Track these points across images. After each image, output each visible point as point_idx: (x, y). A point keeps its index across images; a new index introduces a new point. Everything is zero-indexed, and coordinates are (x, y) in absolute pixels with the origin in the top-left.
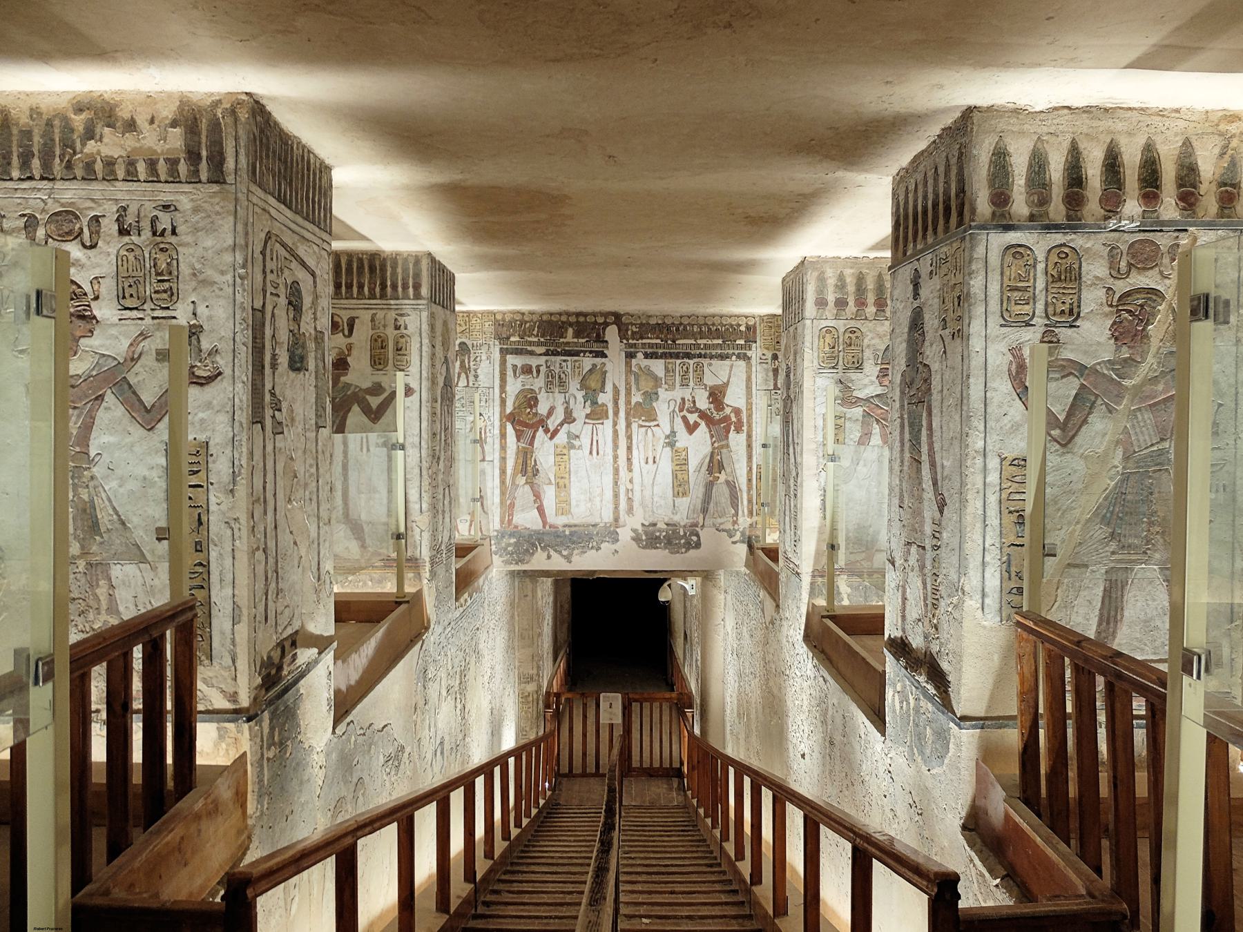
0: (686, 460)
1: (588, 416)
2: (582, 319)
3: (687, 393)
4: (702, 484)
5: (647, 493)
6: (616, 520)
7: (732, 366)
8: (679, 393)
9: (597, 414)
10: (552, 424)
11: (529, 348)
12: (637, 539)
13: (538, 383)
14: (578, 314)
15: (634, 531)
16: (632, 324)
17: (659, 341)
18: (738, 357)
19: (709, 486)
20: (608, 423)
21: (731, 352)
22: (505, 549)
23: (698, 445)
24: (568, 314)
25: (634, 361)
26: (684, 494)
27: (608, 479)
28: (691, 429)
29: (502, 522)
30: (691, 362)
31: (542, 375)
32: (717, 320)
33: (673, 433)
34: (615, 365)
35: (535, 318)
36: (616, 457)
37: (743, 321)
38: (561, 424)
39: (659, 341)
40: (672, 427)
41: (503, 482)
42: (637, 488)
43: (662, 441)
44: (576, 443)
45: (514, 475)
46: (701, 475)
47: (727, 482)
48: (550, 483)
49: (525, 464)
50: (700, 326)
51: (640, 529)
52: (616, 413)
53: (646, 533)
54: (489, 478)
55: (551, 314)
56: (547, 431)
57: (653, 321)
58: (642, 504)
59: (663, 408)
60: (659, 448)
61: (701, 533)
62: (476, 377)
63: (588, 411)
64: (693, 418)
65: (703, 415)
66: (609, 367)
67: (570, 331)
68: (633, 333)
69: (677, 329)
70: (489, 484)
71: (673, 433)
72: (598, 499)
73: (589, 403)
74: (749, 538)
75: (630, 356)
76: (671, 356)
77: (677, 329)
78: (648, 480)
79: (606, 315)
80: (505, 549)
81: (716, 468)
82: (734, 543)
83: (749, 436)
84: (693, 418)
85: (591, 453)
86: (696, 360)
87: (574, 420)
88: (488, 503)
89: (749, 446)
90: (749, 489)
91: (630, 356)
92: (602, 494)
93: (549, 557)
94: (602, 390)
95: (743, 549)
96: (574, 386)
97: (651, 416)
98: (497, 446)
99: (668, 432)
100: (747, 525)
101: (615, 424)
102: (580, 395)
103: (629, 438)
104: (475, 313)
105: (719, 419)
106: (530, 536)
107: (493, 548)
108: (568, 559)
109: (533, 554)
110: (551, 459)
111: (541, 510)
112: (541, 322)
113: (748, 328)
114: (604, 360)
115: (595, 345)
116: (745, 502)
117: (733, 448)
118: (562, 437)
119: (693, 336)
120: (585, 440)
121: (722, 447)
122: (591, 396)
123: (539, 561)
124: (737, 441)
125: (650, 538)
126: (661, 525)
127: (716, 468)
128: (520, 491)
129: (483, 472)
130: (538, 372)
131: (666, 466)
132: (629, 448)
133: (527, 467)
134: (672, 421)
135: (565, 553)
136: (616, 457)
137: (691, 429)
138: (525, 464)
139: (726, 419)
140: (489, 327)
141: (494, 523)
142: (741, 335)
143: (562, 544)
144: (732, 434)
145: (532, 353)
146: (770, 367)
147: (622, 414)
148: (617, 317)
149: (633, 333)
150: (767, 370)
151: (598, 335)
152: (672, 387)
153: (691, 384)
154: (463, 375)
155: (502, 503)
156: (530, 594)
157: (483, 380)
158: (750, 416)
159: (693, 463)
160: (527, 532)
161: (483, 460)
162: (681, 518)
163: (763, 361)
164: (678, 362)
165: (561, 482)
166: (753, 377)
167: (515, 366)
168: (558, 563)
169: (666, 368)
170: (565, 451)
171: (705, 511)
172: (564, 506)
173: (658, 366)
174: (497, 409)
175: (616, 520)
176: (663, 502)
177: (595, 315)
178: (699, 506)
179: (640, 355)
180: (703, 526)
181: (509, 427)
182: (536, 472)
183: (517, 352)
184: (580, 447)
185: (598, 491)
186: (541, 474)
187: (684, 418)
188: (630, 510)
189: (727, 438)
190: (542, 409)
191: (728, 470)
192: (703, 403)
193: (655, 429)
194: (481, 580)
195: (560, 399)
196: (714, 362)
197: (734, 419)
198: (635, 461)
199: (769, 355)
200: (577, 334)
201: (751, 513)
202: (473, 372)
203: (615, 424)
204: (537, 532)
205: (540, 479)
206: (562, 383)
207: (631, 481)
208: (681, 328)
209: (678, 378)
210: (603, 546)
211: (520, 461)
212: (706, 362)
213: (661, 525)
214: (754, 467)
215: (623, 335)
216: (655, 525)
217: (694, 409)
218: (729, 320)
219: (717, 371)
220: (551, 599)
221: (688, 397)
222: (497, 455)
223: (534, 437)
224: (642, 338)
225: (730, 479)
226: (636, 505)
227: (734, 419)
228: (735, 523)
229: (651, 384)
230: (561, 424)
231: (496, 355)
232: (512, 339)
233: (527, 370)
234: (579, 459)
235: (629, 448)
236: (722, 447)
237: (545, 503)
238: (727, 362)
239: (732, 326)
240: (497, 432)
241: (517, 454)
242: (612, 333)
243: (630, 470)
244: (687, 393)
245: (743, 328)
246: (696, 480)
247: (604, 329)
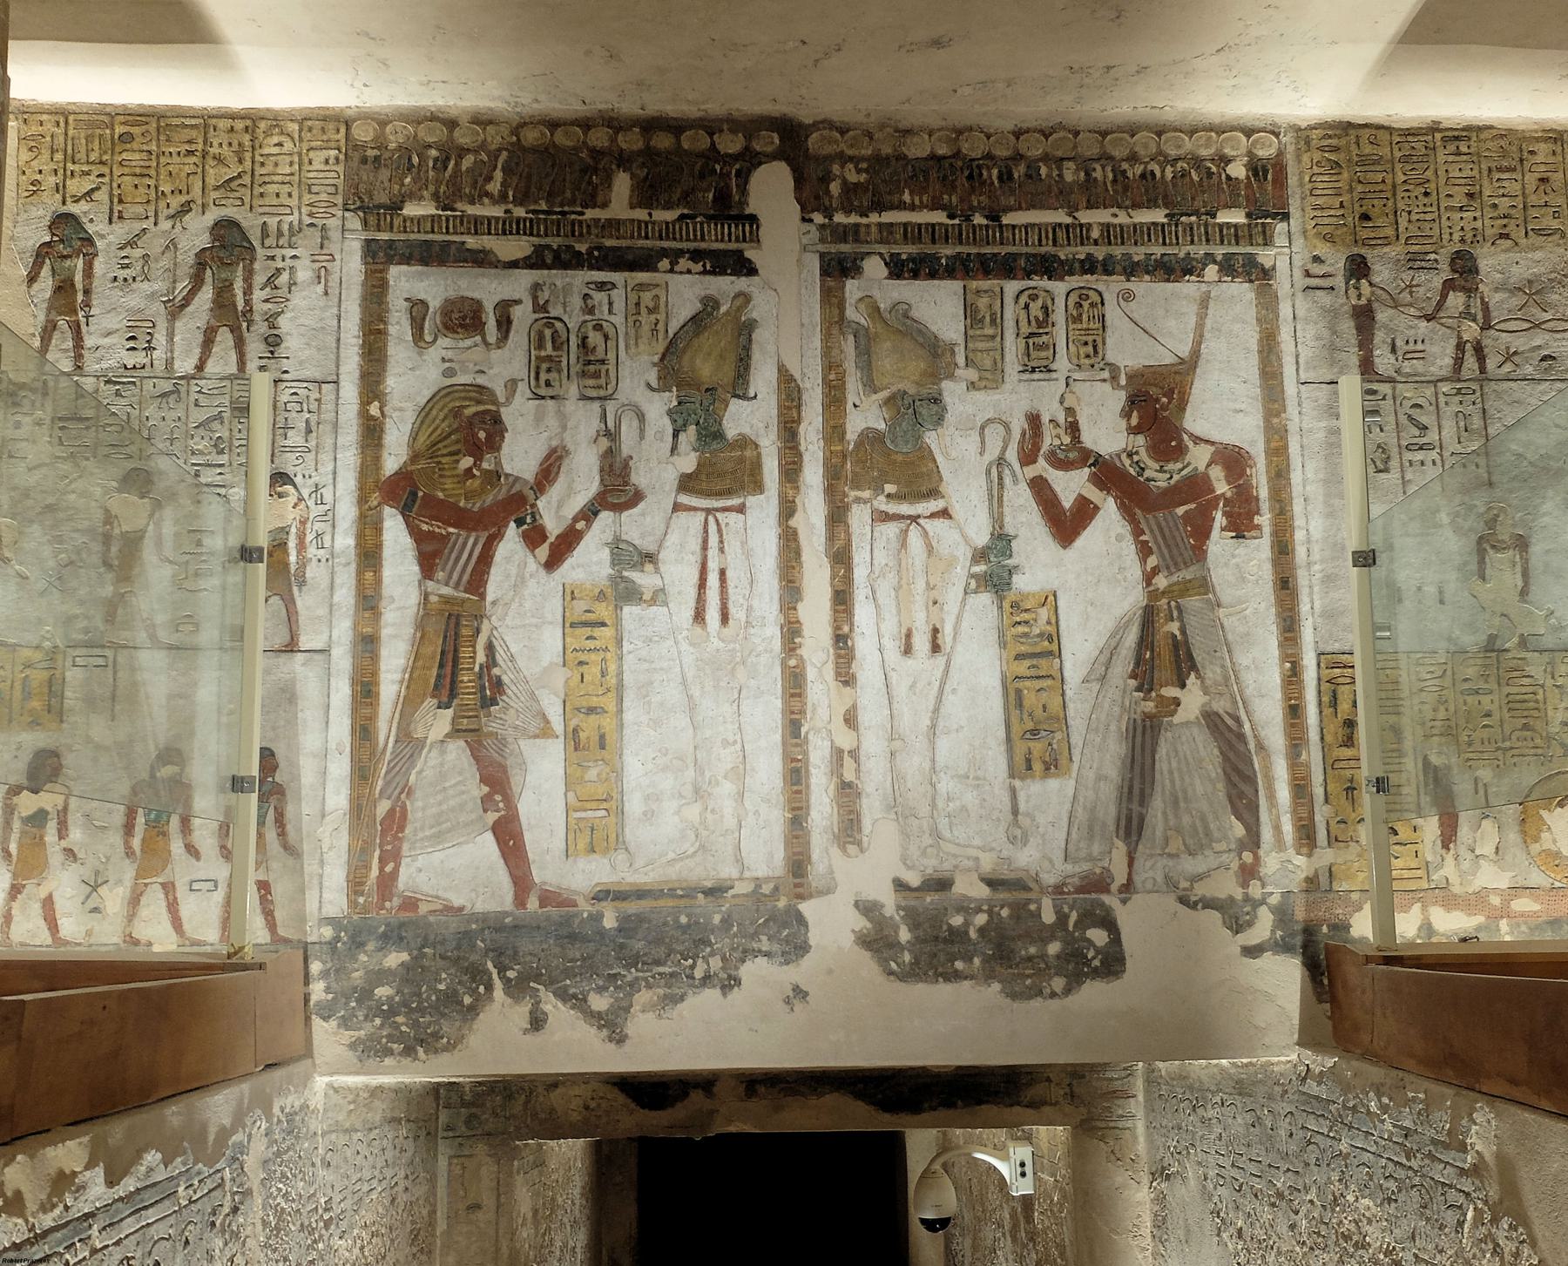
0: (1054, 637)
1: (687, 483)
2: (663, 141)
3: (1047, 399)
4: (1118, 727)
5: (914, 764)
6: (798, 865)
7: (1204, 302)
8: (1016, 397)
9: (721, 475)
10: (554, 511)
11: (471, 242)
12: (877, 942)
13: (505, 365)
14: (650, 125)
15: (867, 908)
16: (843, 159)
17: (939, 217)
18: (1228, 268)
19: (1144, 735)
20: (763, 508)
21: (1200, 250)
22: (365, 994)
23: (1094, 584)
24: (615, 124)
25: (853, 289)
26: (1052, 766)
27: (766, 712)
28: (1067, 524)
29: (355, 884)
30: (1059, 288)
31: (518, 336)
32: (1144, 144)
33: (1001, 541)
34: (783, 304)
35: (495, 137)
36: (792, 632)
37: (1237, 147)
38: (589, 514)
39: (939, 217)
40: (998, 519)
41: (363, 731)
42: (873, 745)
43: (960, 572)
44: (644, 579)
45: (409, 704)
46: (1112, 693)
47: (1212, 720)
48: (546, 732)
49: (450, 660)
50: (1085, 165)
51: (889, 901)
52: (791, 471)
53: (913, 918)
54: (308, 713)
55: (553, 124)
56: (534, 536)
57: (918, 149)
58: (897, 807)
59: (961, 450)
60: (953, 595)
61: (1125, 917)
62: (273, 342)
63: (688, 462)
64: (1071, 485)
65: (1107, 474)
66: (762, 307)
67: (622, 184)
68: (849, 189)
69: (1006, 177)
70: (310, 740)
71: (1001, 541)
72: (728, 787)
73: (689, 436)
74: (1309, 931)
75: (838, 269)
76: (989, 267)
77: (1006, 177)
78: (913, 718)
79: (750, 126)
80: (365, 994)
81: (1165, 671)
82: (1252, 952)
83: (1283, 549)
84: (1071, 485)
85: (699, 616)
86: (1075, 281)
87: (637, 497)
88: (302, 810)
89: (1285, 584)
90: (1296, 742)
91: (838, 269)
92: (740, 772)
93: (537, 1022)
94: (739, 386)
95: (1282, 982)
96: (635, 375)
97: (919, 480)
98: (345, 595)
99: (982, 539)
100: (1295, 882)
101: (788, 509)
102: (658, 408)
103: (841, 558)
104: (275, 120)
105: (1169, 494)
106: (466, 937)
107: (318, 990)
108: (612, 1026)
109: (473, 1011)
110: (551, 641)
111: (509, 836)
112: (517, 150)
113: (1257, 169)
114: (742, 283)
115: (712, 230)
116: (1284, 794)
117: (1225, 593)
118: (590, 561)
119: (1062, 196)
120: (678, 571)
121: (1185, 589)
122: (699, 409)
123: (505, 1040)
124: (1237, 565)
125: (929, 937)
126: (970, 888)
127: (1165, 671)
128: (427, 766)
129: (286, 696)
130: (505, 323)
131: (979, 662)
132: (842, 599)
133: (457, 668)
134: (996, 498)
135: (599, 1003)
136: (792, 632)
137: (1067, 524)
138: (450, 660)
139: (1195, 487)
140: (325, 167)
141: (326, 891)
142: (1232, 193)
143: (589, 967)
144: (1219, 544)
145: (481, 260)
146: (1344, 301)
147: (813, 475)
148: (791, 139)
149: (849, 189)
150: (1332, 314)
151: (723, 198)
152: (991, 378)
153: (1062, 364)
154: (224, 338)
155: (359, 809)
156: (488, 1200)
157: (300, 352)
158: (1280, 475)
159: (1080, 649)
160: (454, 924)
161: (291, 648)
162: (1045, 856)
163: (1314, 283)
164: (1011, 287)
165: (589, 727)
166: (1285, 335)
167: (417, 309)
168: (570, 1045)
169: (970, 311)
170: (603, 611)
171: (1131, 828)
172: (598, 820)
173: (939, 306)
174: (349, 458)
175: (798, 865)
176: (970, 798)
177: (710, 126)
178: (1109, 812)
179: (874, 268)
180: (1128, 888)
181: (395, 532)
182: (491, 691)
183: (428, 255)
184: (659, 597)
185: (728, 757)
186: (514, 696)
187: (1042, 490)
188: (849, 830)
189: (1200, 554)
190: (519, 457)
191: (1212, 673)
192: (1107, 432)
193: (936, 527)
194: (218, 1106)
195: (582, 422)
196: (1143, 287)
197: (1222, 488)
198: (864, 645)
199: (1336, 261)
200: (646, 195)
201: (1306, 836)
202: (261, 328)
203: (788, 509)
204: (493, 924)
205: (507, 718)
206: (594, 369)
207: (851, 720)
208: (1019, 171)
209: (1013, 346)
210: (751, 970)
211: (434, 648)
212: (1110, 287)
213: (970, 888)
214: (1309, 661)
215: (811, 197)
216: (942, 884)
217: (1075, 455)
218: (1188, 145)
219: (1152, 321)
220: (580, 1239)
221: (1051, 410)
222: (343, 630)
223: (485, 560)
224: (880, 207)
225: (1220, 706)
226: (871, 807)
227: (1222, 488)
228: (1249, 873)
229: (917, 365)
230: (589, 514)
231: (351, 264)
232: (411, 210)
233: (463, 319)
234: (656, 639)
235: (842, 599)
236: (1185, 589)
237: (526, 808)
238: (1188, 288)
239: (1197, 162)
240: (345, 541)
241: (421, 625)
242: (771, 190)
243: (846, 678)
244: (1047, 399)
245: (1238, 170)
246: (1092, 708)
247: (744, 177)
